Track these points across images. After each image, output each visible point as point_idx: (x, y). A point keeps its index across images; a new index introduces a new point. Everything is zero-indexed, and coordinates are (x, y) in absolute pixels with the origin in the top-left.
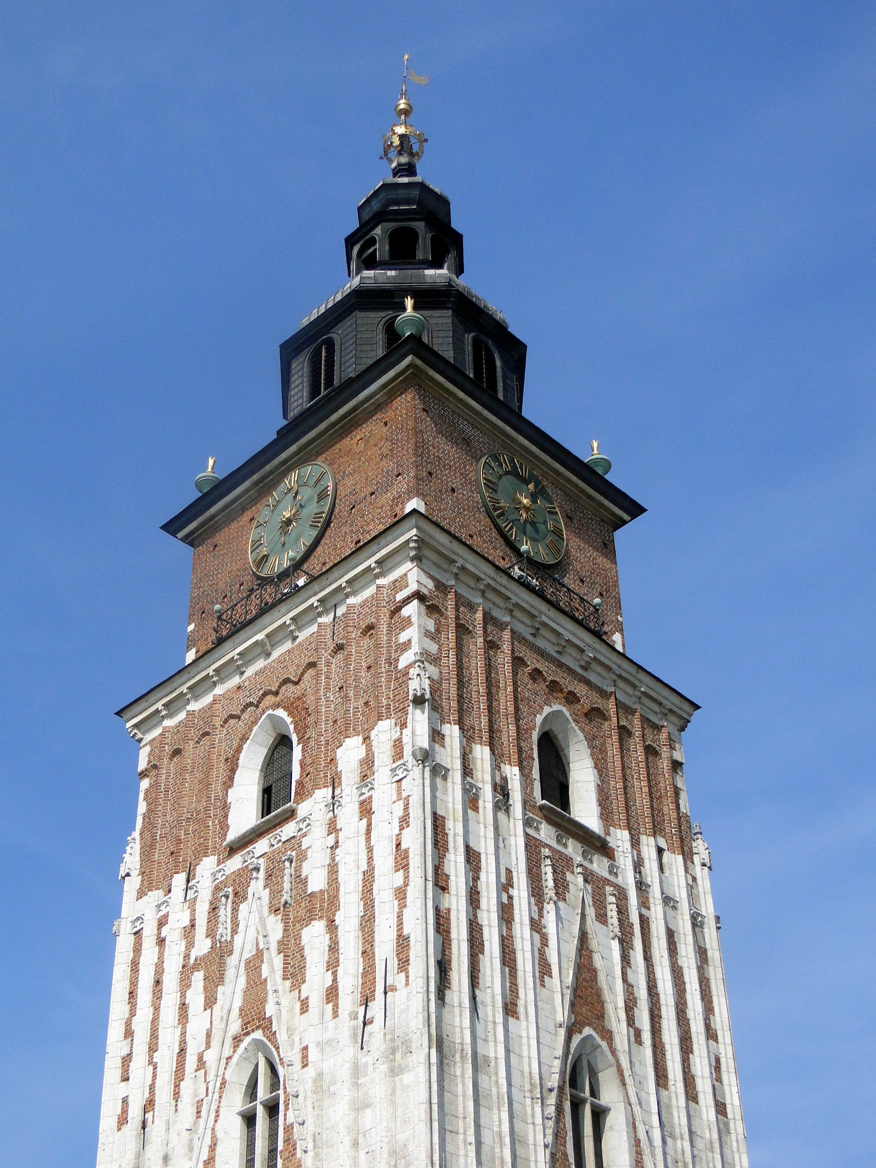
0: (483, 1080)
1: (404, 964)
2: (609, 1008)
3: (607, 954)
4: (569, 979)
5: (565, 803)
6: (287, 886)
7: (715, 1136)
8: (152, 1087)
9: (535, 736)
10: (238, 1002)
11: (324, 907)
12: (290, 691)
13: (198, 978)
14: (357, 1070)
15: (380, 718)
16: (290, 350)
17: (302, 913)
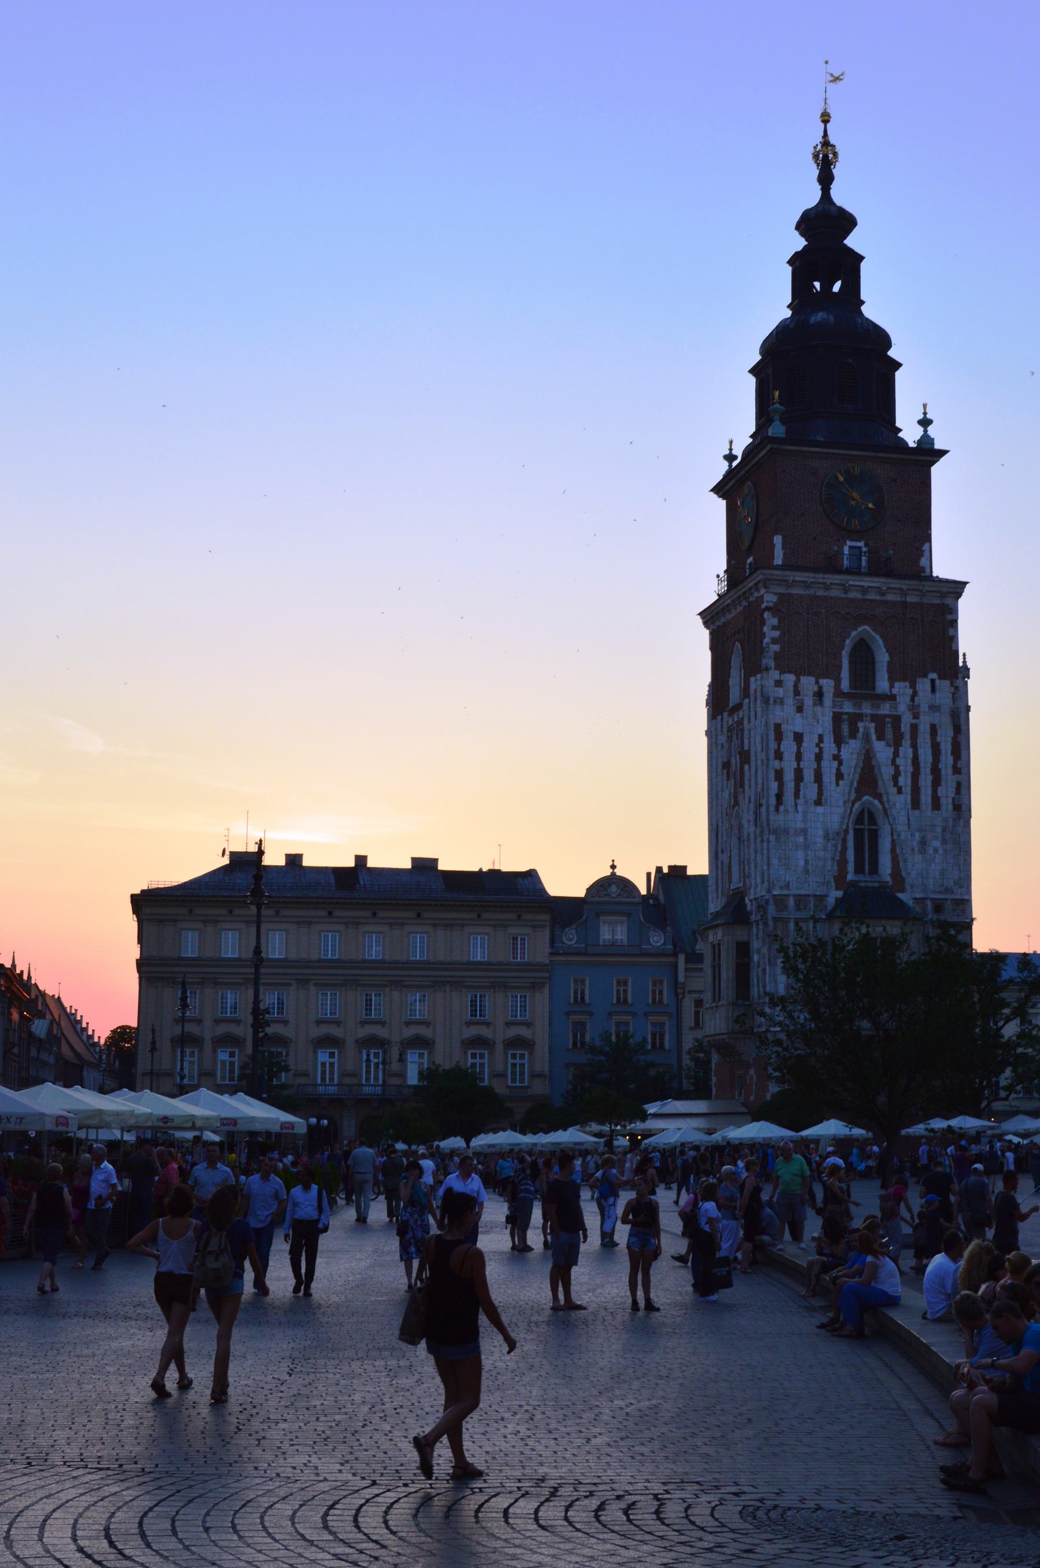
2: (880, 783)
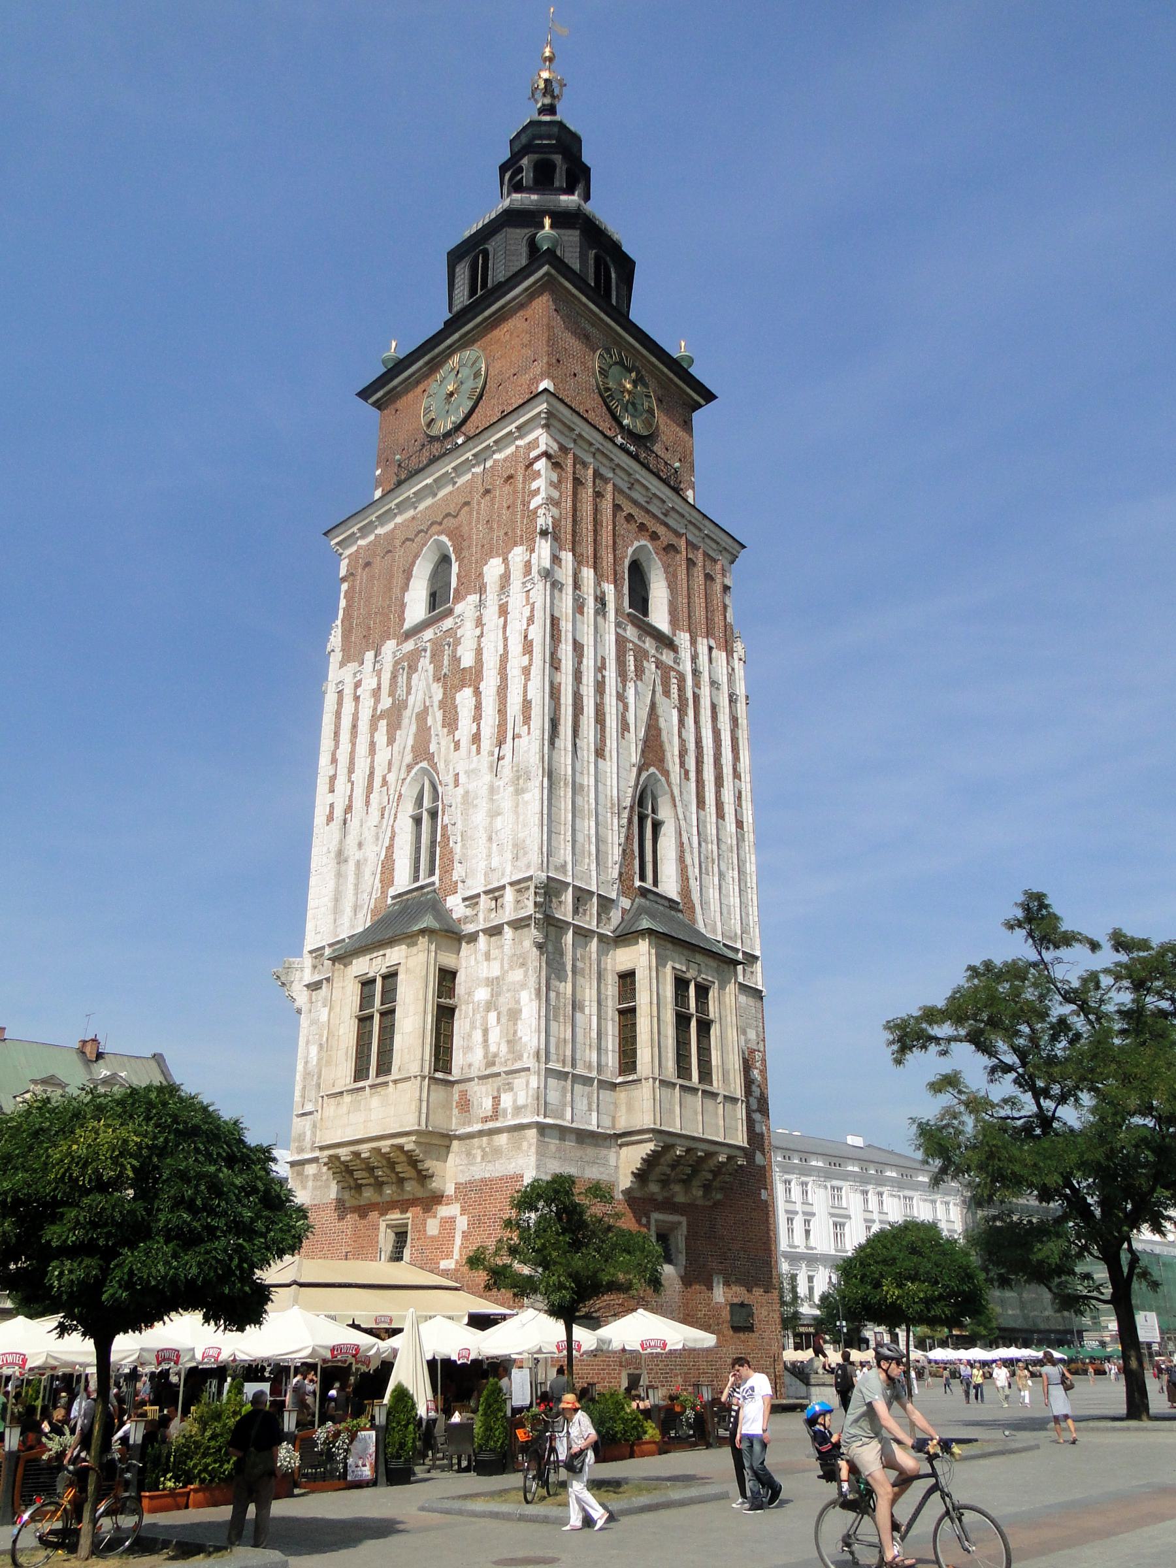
0: (579, 799)
1: (527, 719)
2: (668, 755)
3: (669, 718)
4: (642, 734)
5: (645, 612)
6: (446, 662)
7: (735, 842)
8: (351, 797)
9: (627, 563)
10: (410, 742)
11: (473, 677)
12: (450, 523)
13: (383, 724)
14: (492, 790)
15: (515, 544)
16: (455, 257)
17: (456, 682)
